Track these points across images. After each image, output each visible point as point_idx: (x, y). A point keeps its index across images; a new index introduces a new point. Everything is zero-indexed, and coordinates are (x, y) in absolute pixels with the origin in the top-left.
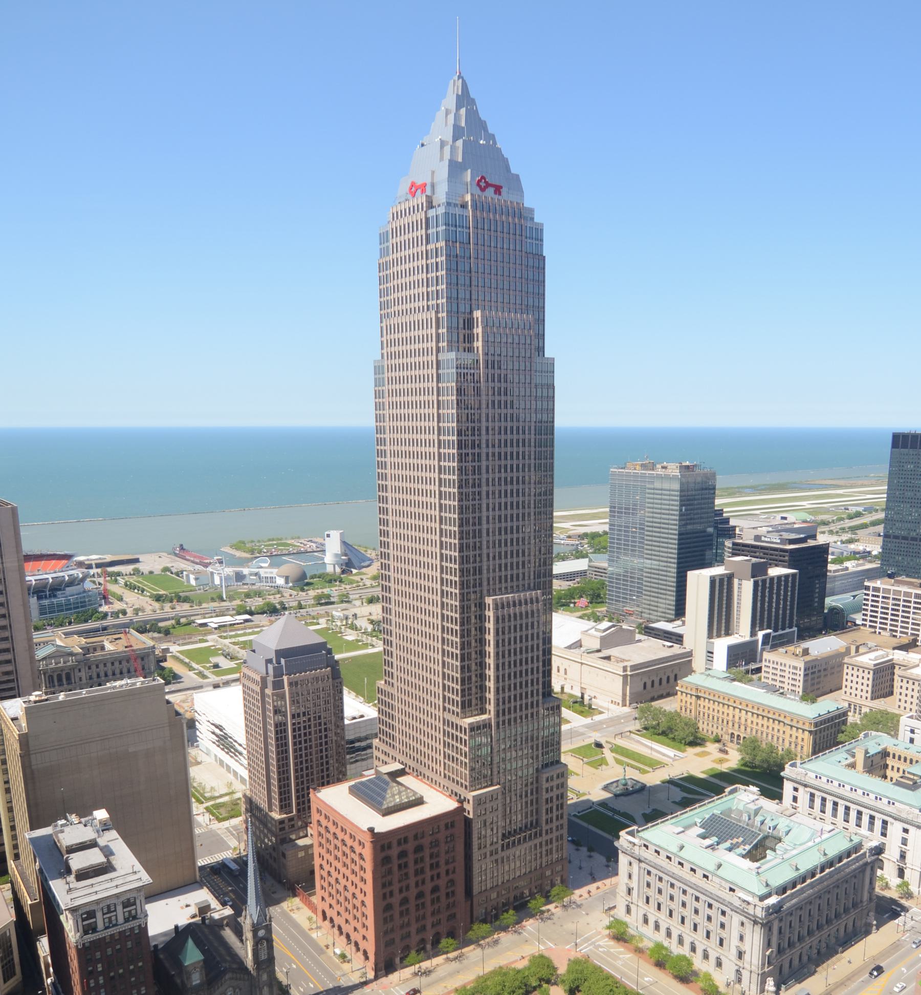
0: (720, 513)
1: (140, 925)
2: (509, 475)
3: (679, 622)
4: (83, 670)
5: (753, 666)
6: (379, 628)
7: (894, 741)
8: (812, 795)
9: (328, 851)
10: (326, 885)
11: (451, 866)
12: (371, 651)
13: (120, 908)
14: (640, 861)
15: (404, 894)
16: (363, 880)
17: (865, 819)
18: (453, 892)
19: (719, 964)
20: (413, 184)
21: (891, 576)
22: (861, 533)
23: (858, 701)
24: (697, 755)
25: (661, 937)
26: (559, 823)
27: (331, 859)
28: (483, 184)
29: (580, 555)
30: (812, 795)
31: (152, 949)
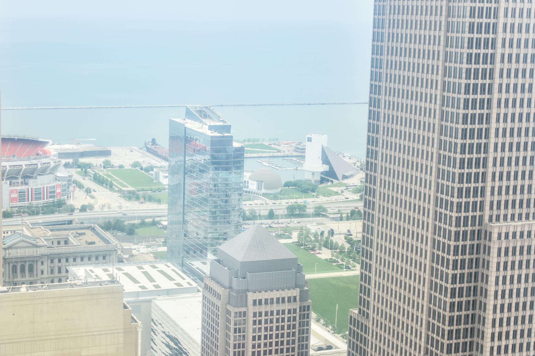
4: (45, 263)
6: (360, 251)
12: (345, 273)
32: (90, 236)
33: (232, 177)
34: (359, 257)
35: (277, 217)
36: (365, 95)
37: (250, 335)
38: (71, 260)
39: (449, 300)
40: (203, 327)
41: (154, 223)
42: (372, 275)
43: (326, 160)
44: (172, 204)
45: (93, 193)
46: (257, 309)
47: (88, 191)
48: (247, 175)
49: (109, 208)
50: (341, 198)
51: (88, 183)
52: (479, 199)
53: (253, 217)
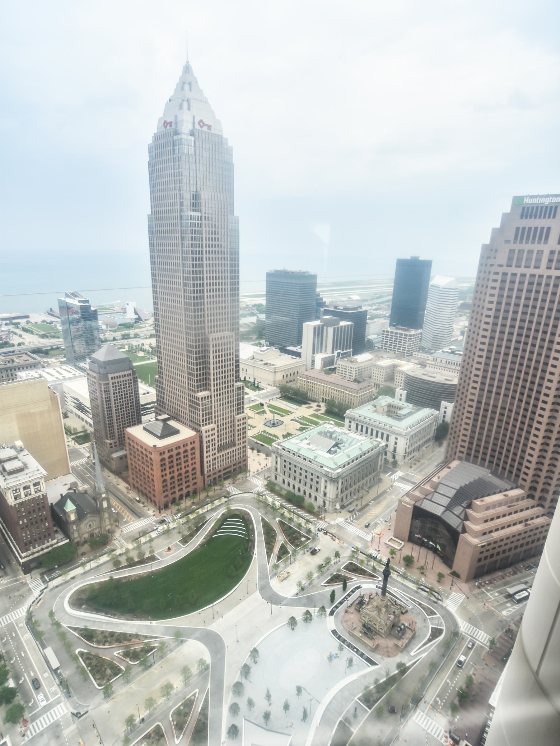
0: (319, 295)
1: (43, 495)
2: (217, 275)
3: (300, 347)
5: (333, 367)
6: (156, 351)
7: (393, 400)
8: (357, 425)
9: (135, 457)
10: (134, 472)
11: (194, 461)
13: (32, 487)
14: (281, 456)
15: (172, 475)
16: (152, 470)
17: (380, 434)
18: (195, 473)
19: (316, 499)
20: (165, 122)
21: (394, 326)
22: (383, 305)
23: (378, 382)
24: (307, 408)
25: (291, 489)
26: (244, 440)
27: (136, 460)
28: (201, 124)
29: (253, 314)
30: (357, 425)
31: (50, 505)
32: (25, 357)
33: (93, 324)
34: (156, 354)
35: (117, 340)
36: (150, 283)
37: (112, 392)
38: (17, 369)
39: (195, 367)
40: (89, 392)
41: (58, 348)
42: (163, 361)
43: (136, 313)
44: (65, 339)
45: (23, 337)
46: (114, 381)
47: (20, 336)
48: (100, 323)
49: (33, 343)
50: (145, 329)
51: (19, 331)
52: (203, 325)
53: (106, 341)
